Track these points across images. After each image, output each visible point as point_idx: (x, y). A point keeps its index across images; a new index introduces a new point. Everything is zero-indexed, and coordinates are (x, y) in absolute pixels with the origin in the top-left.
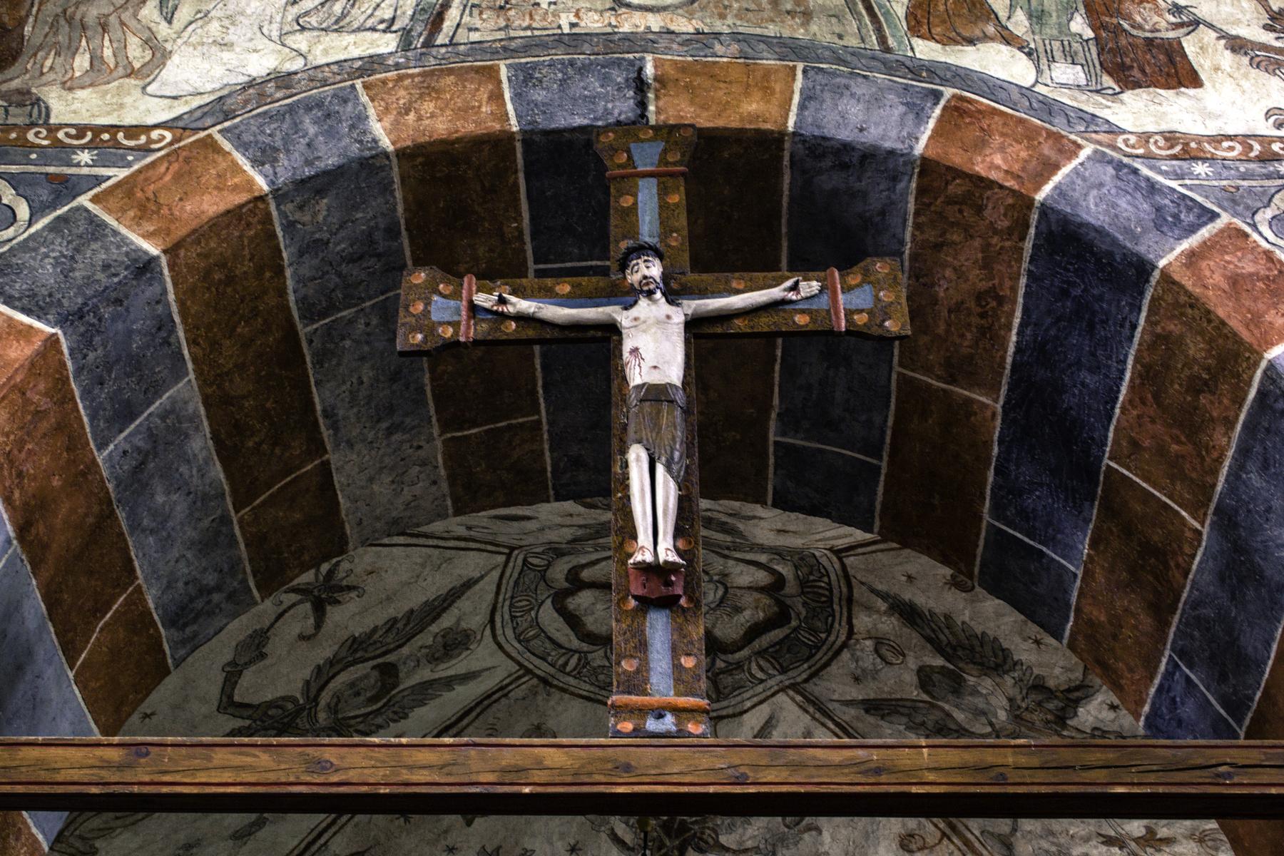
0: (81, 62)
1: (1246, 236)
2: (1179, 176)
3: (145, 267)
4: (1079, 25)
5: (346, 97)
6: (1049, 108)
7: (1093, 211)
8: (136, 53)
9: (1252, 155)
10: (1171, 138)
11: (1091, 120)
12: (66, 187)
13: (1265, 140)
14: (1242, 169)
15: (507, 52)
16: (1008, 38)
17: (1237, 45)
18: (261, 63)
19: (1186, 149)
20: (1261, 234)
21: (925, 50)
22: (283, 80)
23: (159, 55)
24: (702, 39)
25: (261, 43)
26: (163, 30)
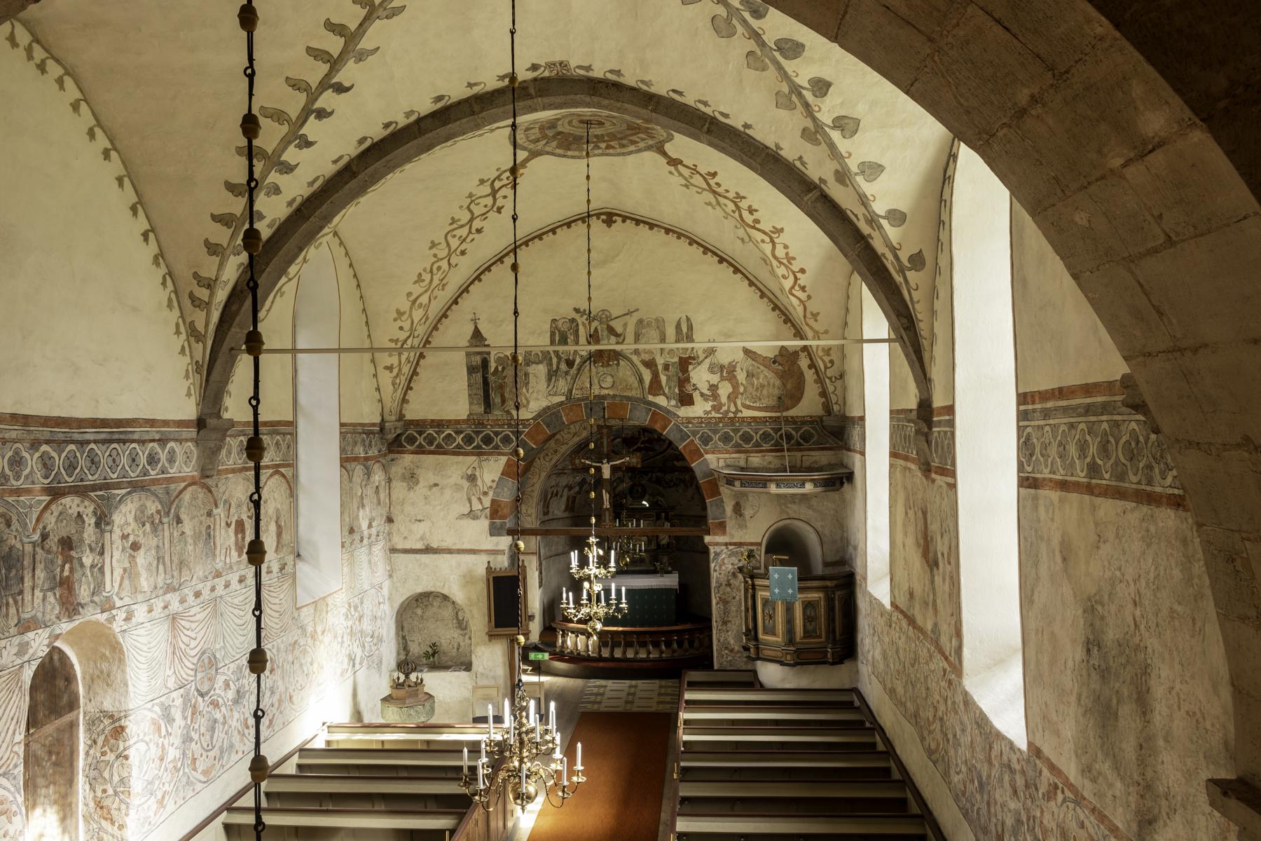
6: (668, 412)
7: (671, 438)
16: (664, 394)
17: (702, 395)
19: (689, 420)
21: (650, 398)
22: (548, 408)
23: (528, 403)
24: (615, 396)
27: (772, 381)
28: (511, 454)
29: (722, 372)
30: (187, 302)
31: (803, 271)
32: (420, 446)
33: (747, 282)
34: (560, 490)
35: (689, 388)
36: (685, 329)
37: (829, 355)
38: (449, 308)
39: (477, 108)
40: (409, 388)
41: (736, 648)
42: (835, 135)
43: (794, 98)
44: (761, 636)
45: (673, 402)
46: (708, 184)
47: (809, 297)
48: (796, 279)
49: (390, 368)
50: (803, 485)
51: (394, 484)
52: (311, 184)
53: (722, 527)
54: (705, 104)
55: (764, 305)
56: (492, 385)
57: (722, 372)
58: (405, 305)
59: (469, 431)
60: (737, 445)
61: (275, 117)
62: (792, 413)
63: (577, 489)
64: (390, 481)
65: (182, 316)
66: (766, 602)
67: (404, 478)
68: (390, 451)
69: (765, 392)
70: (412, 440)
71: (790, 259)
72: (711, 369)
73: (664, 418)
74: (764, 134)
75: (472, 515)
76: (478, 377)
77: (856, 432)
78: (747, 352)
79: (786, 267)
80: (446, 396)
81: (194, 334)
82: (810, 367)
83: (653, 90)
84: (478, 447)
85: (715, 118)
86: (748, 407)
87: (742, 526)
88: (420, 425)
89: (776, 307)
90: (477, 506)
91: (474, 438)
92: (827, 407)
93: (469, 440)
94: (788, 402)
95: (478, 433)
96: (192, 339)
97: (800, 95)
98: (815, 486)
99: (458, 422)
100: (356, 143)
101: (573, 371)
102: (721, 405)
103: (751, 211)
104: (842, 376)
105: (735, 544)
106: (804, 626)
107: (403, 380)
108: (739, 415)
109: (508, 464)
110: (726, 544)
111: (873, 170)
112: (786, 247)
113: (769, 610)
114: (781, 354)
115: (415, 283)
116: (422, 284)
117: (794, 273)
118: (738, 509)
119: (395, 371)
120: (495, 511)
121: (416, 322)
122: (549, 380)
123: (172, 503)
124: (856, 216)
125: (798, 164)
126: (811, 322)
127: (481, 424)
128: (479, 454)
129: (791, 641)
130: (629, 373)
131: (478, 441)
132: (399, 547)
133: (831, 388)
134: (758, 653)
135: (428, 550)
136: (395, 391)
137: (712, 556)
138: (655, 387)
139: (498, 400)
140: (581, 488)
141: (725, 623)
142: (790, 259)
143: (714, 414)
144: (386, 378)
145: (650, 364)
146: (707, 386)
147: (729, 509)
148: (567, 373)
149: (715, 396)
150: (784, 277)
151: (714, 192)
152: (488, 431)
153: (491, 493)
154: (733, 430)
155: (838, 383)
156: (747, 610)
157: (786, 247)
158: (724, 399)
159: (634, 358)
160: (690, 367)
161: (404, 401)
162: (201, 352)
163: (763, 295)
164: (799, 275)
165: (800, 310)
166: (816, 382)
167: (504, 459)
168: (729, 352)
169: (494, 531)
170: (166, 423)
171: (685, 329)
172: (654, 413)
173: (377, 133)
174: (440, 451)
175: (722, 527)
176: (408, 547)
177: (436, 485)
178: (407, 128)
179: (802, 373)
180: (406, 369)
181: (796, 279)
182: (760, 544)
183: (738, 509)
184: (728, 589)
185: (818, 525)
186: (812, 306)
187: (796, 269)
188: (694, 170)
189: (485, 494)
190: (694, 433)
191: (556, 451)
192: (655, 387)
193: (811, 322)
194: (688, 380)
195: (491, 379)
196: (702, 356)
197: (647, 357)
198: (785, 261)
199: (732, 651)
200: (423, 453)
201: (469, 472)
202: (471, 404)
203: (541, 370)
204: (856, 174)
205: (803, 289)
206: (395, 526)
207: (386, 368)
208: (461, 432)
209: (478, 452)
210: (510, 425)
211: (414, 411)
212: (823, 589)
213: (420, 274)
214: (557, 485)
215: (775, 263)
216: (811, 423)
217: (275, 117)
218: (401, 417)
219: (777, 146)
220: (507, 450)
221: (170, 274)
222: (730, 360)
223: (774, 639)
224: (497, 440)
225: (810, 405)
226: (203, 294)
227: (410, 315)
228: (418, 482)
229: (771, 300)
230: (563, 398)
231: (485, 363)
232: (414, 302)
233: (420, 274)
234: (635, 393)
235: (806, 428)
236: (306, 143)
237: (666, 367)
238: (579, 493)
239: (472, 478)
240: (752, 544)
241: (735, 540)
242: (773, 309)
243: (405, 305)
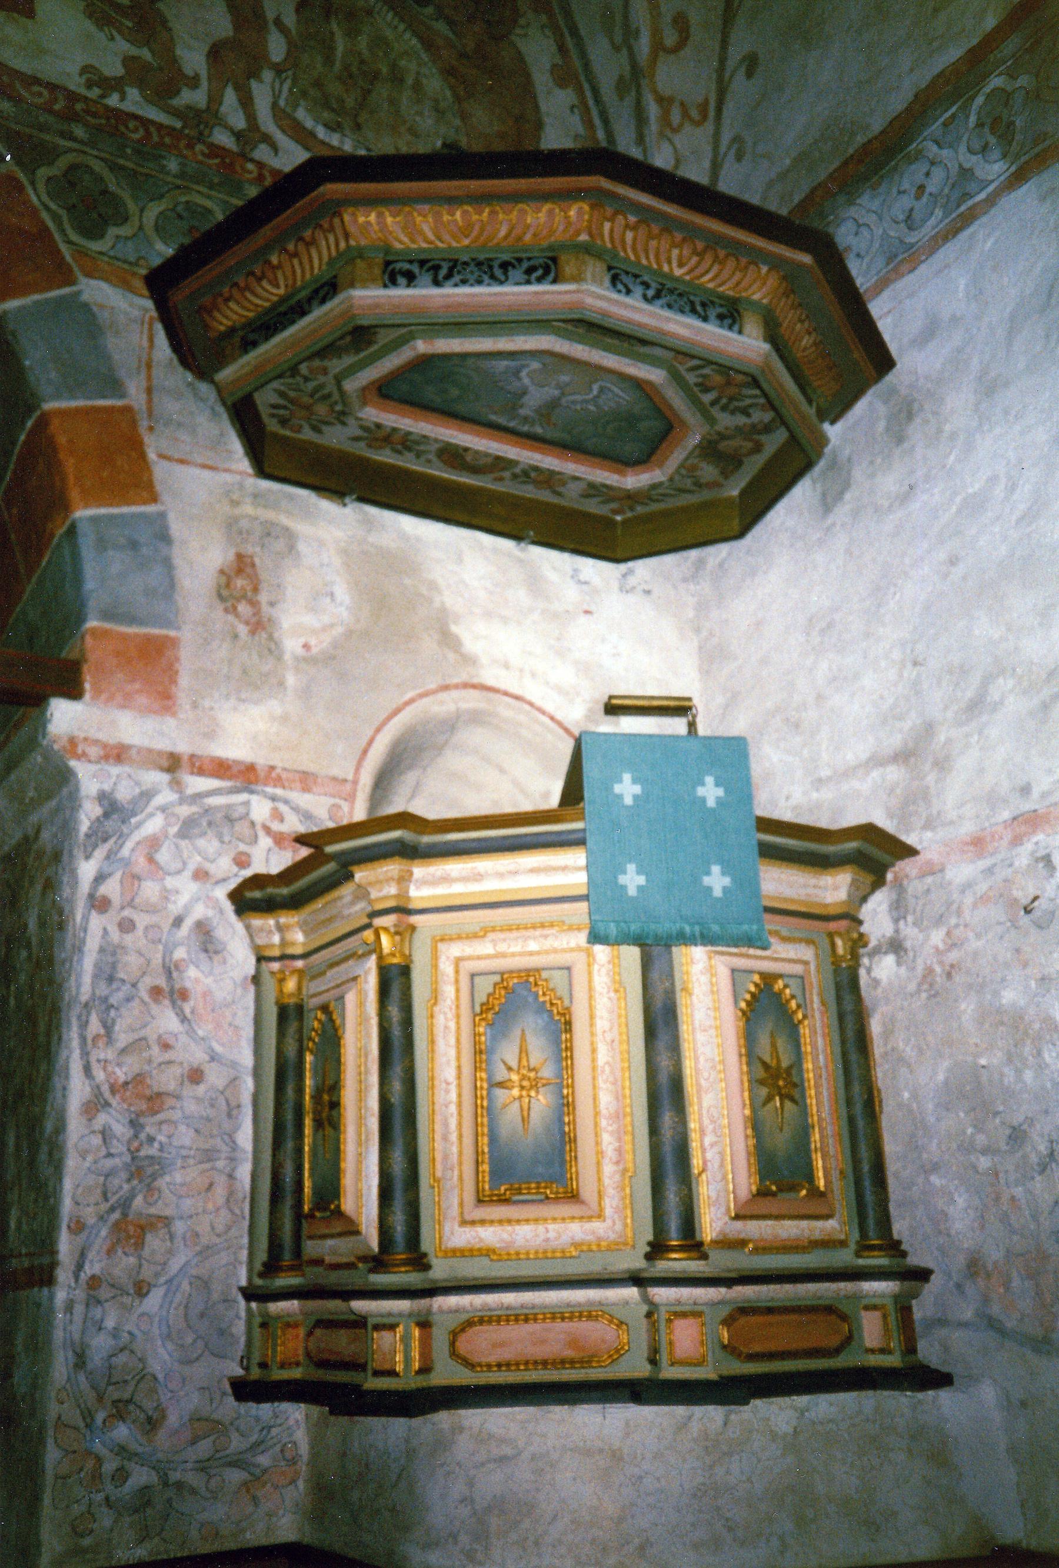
1: (21, 189)
9: (57, 107)
13: (72, 97)
14: (42, 119)
20: (35, 190)
53: (152, 666)
82: (563, 77)
105: (221, 768)
108: (262, 152)
110: (172, 764)
113: (526, 1045)
137: (88, 813)
175: (152, 666)
182: (343, 787)
183: (242, 585)
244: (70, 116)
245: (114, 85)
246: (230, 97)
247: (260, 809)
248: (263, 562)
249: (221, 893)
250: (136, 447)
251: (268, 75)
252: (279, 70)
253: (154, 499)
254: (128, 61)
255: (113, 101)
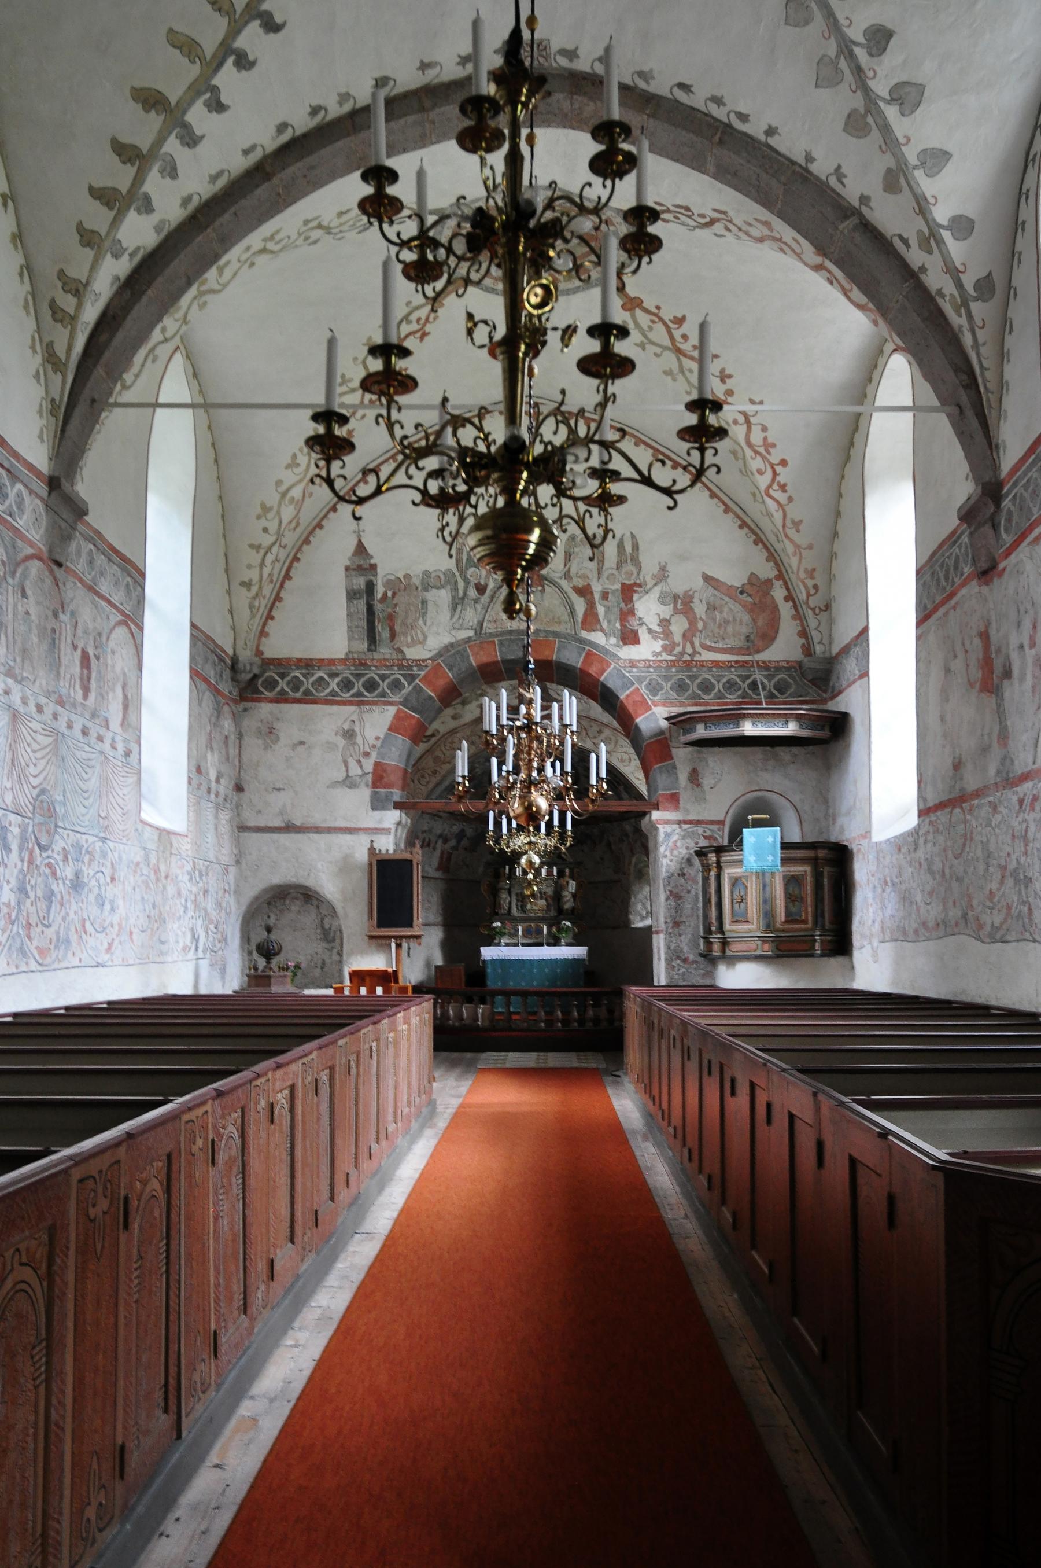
0: (409, 639)
2: (629, 672)
3: (431, 697)
4: (618, 625)
5: (465, 650)
6: (607, 652)
7: (610, 684)
8: (421, 637)
10: (630, 661)
11: (615, 655)
12: (413, 677)
13: (649, 661)
15: (497, 636)
16: (602, 630)
17: (650, 631)
18: (446, 639)
19: (633, 664)
21: (584, 634)
22: (452, 645)
23: (425, 637)
25: (446, 634)
26: (425, 629)
27: (738, 616)
28: (401, 703)
29: (675, 603)
30: (46, 313)
31: (784, 463)
32: (283, 692)
33: (707, 493)
34: (433, 839)
35: (633, 623)
36: (628, 549)
37: (812, 578)
38: (325, 516)
39: (427, 103)
40: (270, 617)
41: (691, 957)
42: (891, 112)
43: (843, 64)
44: (727, 926)
45: (613, 640)
46: (672, 338)
47: (790, 499)
48: (775, 474)
49: (247, 585)
50: (787, 723)
51: (247, 740)
52: (214, 179)
54: (718, 101)
55: (729, 522)
56: (379, 614)
57: (675, 603)
58: (273, 500)
59: (347, 674)
60: (695, 696)
61: (185, 49)
62: (767, 655)
63: (453, 843)
64: (240, 736)
65: (39, 330)
66: (736, 881)
67: (259, 733)
68: (242, 698)
69: (730, 629)
70: (271, 684)
71: (768, 446)
72: (662, 600)
73: (602, 660)
74: (791, 144)
75: (349, 782)
76: (361, 605)
77: (850, 666)
78: (707, 579)
79: (763, 458)
80: (321, 628)
81: (52, 359)
82: (787, 599)
83: (653, 88)
84: (359, 694)
85: (729, 126)
86: (709, 648)
87: (701, 799)
88: (282, 665)
89: (743, 525)
90: (355, 770)
91: (358, 683)
92: (808, 650)
93: (347, 685)
94: (759, 643)
95: (358, 676)
96: (49, 367)
97: (851, 55)
98: (801, 726)
99: (332, 662)
100: (273, 130)
101: (485, 598)
102: (674, 645)
103: (724, 377)
104: (828, 607)
105: (690, 822)
106: (786, 907)
107: (263, 604)
108: (697, 658)
109: (397, 717)
110: (679, 822)
111: (936, 159)
112: (764, 429)
114: (750, 583)
115: (288, 467)
116: (297, 470)
117: (772, 466)
118: (694, 777)
119: (255, 589)
120: (379, 777)
121: (285, 522)
122: (454, 608)
123: (18, 564)
124: (905, 242)
125: (833, 181)
126: (791, 533)
127: (363, 664)
128: (360, 704)
129: (769, 926)
130: (557, 602)
131: (359, 686)
132: (251, 823)
133: (812, 622)
134: (724, 951)
135: (289, 828)
136: (253, 616)
138: (591, 620)
139: (385, 634)
140: (459, 842)
141: (677, 924)
142: (768, 446)
143: (665, 656)
144: (243, 597)
145: (584, 591)
146: (656, 620)
147: (683, 776)
148: (476, 601)
149: (667, 634)
150: (760, 472)
151: (679, 351)
152: (372, 674)
153: (374, 755)
154: (689, 677)
155: (824, 616)
156: (707, 902)
157: (764, 429)
158: (678, 638)
159: (564, 584)
160: (636, 596)
161: (263, 633)
162: (61, 385)
163: (727, 510)
164: (779, 469)
165: (778, 517)
166: (794, 618)
167: (392, 710)
168: (685, 578)
169: (377, 804)
170: (16, 455)
171: (628, 549)
172: (589, 654)
173: (302, 123)
174: (308, 699)
175: (674, 799)
176: (262, 824)
177: (302, 743)
178: (338, 121)
179: (775, 608)
180: (267, 590)
181: (775, 474)
182: (722, 823)
183: (694, 777)
184: (682, 881)
185: (796, 798)
186: (794, 512)
187: (775, 461)
188: (656, 315)
189: (367, 754)
190: (640, 680)
191: (435, 772)
192: (591, 620)
193: (791, 533)
194: (632, 612)
195: (378, 607)
196: (650, 583)
197: (580, 583)
198: (762, 450)
199: (685, 960)
200: (286, 701)
201: (346, 727)
202: (351, 639)
203: (444, 596)
204: (915, 167)
205: (783, 488)
206: (245, 796)
207: (243, 584)
208: (337, 675)
209: (359, 701)
210: (401, 667)
211: (277, 647)
212: (814, 862)
213: (295, 456)
214: (430, 831)
215: (749, 453)
216: (788, 669)
217: (185, 49)
218: (259, 653)
219: (809, 158)
220: (397, 698)
221: (28, 267)
222: (686, 588)
223: (746, 928)
224: (384, 686)
225: (784, 648)
226: (68, 303)
227: (278, 513)
228: (278, 739)
229: (738, 517)
230: (471, 633)
231: (370, 587)
232: (284, 495)
233: (295, 456)
234: (564, 628)
235: (781, 676)
236: (218, 106)
237: (605, 595)
238: (455, 848)
239: (349, 735)
240: (712, 822)
241: (691, 817)
242: (741, 527)
243: (273, 500)
244: (650, 666)
245: (659, 654)
246: (688, 644)
247: (700, 830)
248: (700, 771)
249: (692, 851)
250: (668, 747)
251: (698, 634)
252: (701, 631)
253: (672, 758)
254: (662, 646)
255: (660, 658)
